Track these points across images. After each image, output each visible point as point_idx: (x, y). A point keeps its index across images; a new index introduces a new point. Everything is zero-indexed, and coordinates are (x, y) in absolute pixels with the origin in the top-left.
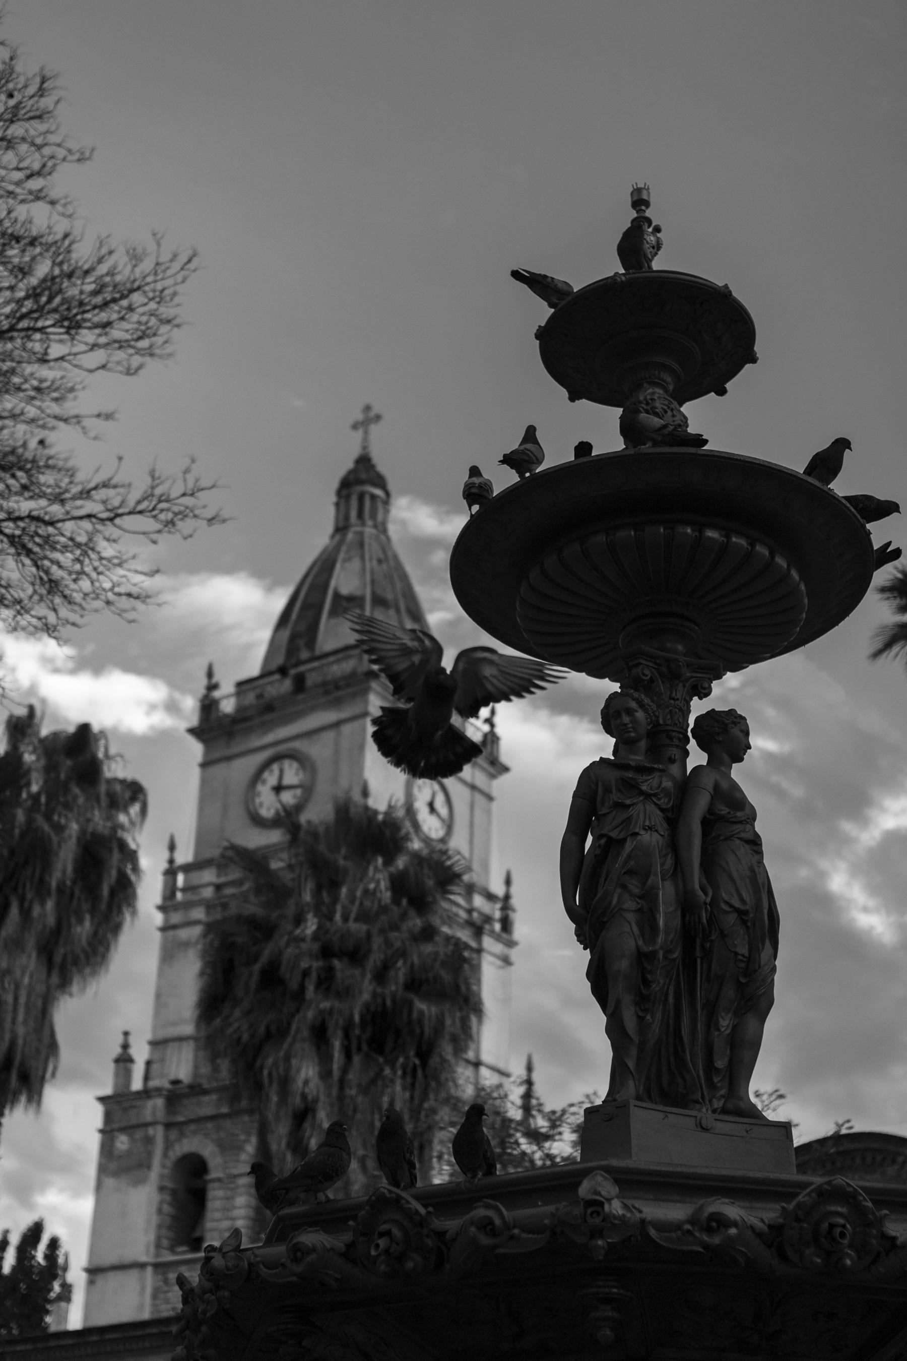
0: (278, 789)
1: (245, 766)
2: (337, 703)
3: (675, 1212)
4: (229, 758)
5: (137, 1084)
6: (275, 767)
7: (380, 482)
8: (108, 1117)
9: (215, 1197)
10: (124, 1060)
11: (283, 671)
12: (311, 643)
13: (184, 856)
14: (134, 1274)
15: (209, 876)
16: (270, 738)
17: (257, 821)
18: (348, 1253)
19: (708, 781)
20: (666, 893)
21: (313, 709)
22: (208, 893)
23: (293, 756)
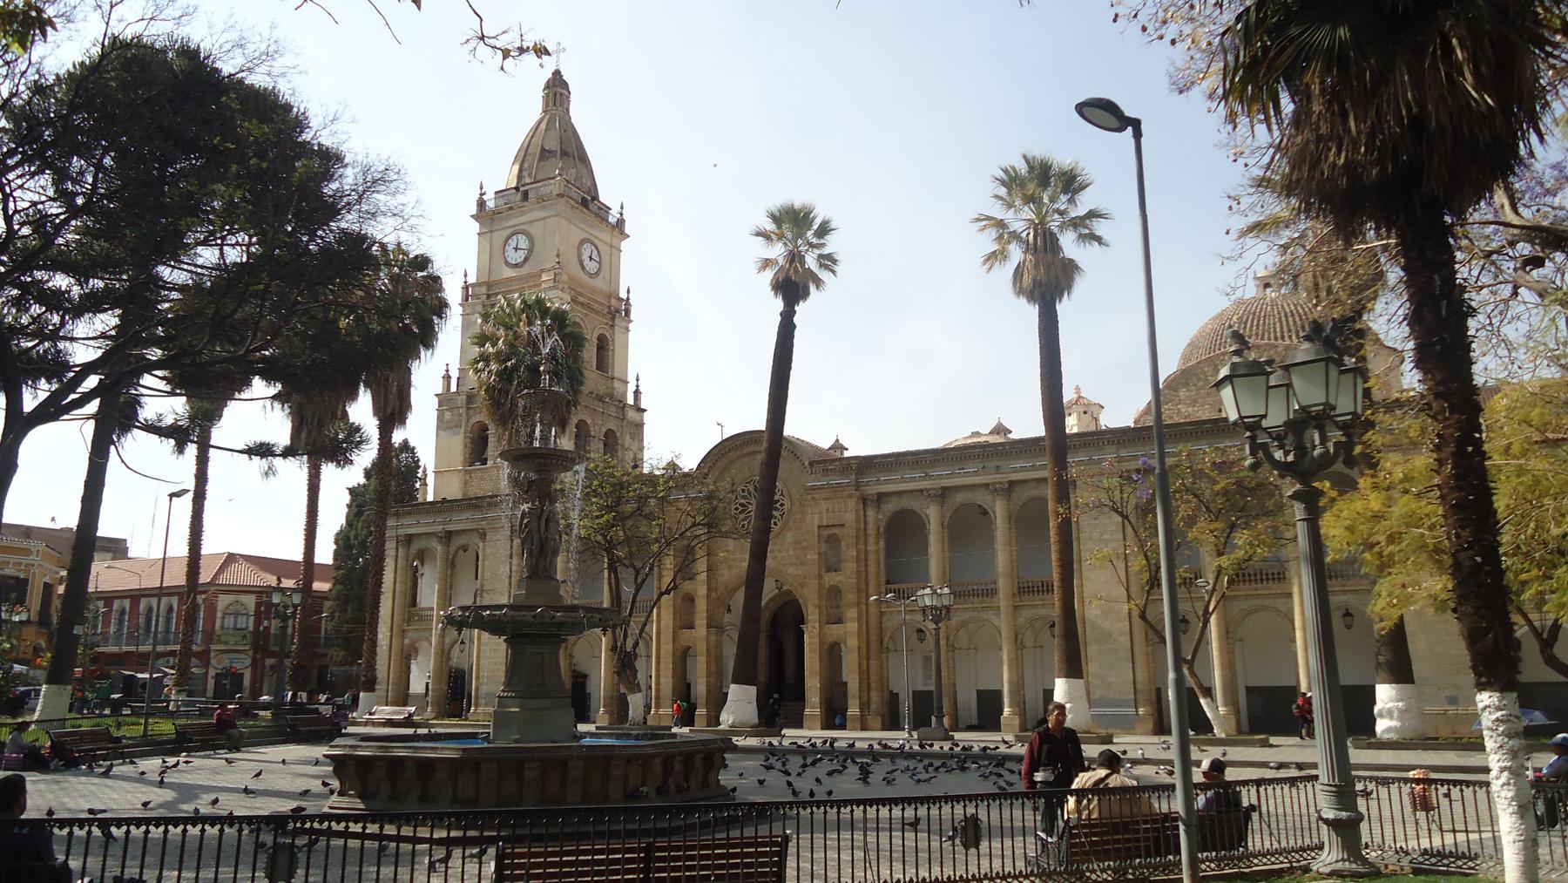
1: (499, 236)
5: (453, 388)
7: (565, 85)
8: (440, 404)
10: (447, 378)
13: (472, 279)
21: (530, 211)
23: (524, 233)
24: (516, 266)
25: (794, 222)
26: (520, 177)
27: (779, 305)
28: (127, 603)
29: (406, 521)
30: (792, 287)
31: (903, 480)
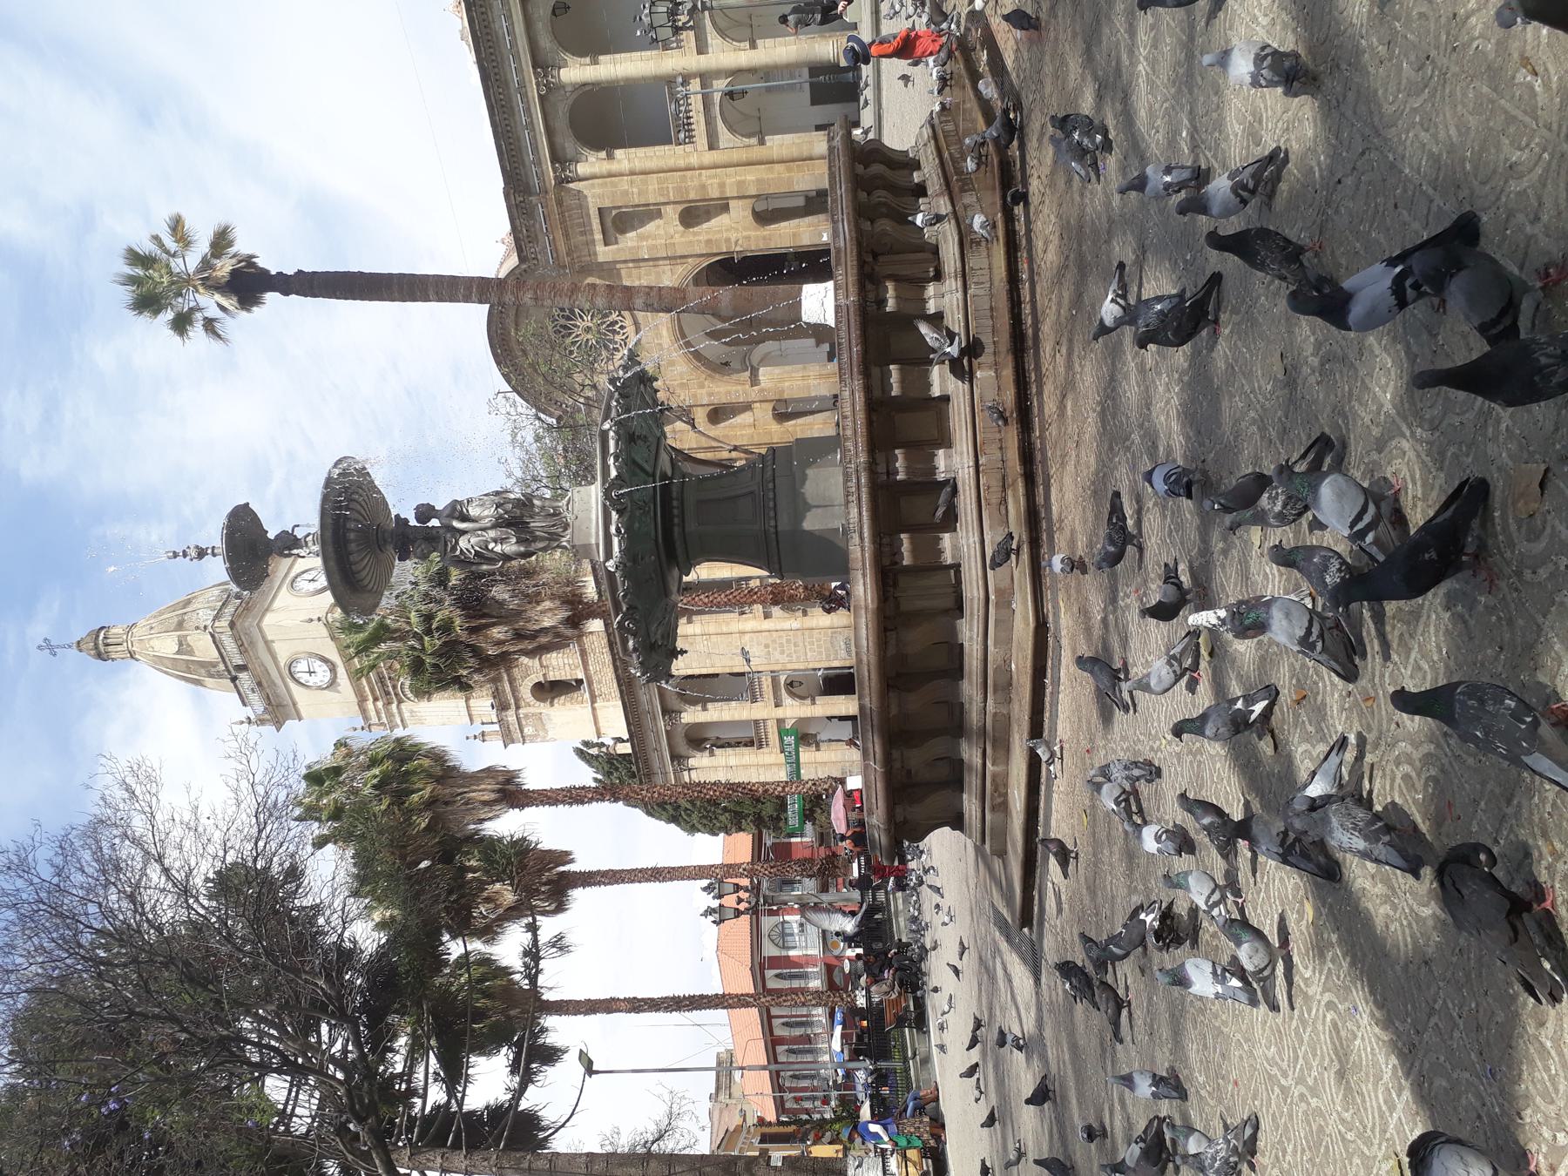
0: (310, 673)
2: (252, 643)
3: (616, 541)
4: (294, 704)
6: (297, 676)
9: (552, 676)
11: (234, 679)
12: (214, 665)
14: (599, 713)
15: (370, 705)
16: (279, 682)
17: (332, 684)
18: (635, 635)
19: (446, 521)
20: (492, 534)
22: (380, 704)
24: (333, 669)
25: (152, 289)
26: (220, 676)
27: (271, 297)
28: (780, 1049)
29: (656, 764)
30: (249, 285)
31: (531, 126)
